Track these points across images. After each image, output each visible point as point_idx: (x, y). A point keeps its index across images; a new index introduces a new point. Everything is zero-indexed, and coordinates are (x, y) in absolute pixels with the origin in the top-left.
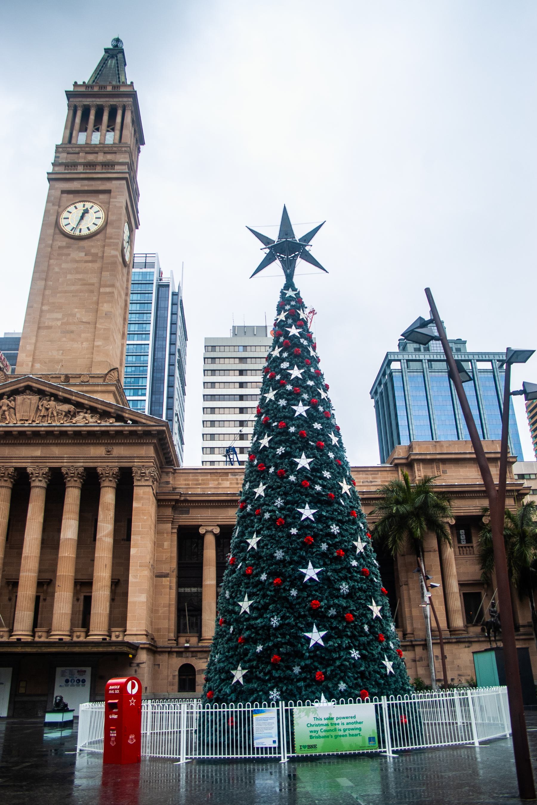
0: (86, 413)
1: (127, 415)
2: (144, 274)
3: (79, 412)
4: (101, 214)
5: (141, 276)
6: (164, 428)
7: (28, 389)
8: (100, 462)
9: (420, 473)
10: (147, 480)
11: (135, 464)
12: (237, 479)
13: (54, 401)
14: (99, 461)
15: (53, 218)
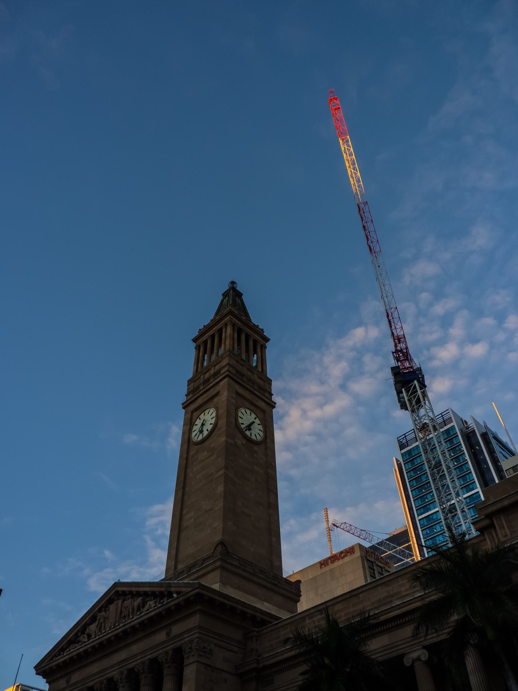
0: (151, 600)
1: (173, 589)
2: (447, 431)
3: (147, 602)
4: (214, 415)
5: (445, 435)
6: (198, 590)
7: (117, 594)
8: (162, 649)
9: (503, 532)
10: (193, 655)
11: (186, 640)
12: (314, 622)
13: (131, 598)
14: (160, 648)
15: (187, 436)
